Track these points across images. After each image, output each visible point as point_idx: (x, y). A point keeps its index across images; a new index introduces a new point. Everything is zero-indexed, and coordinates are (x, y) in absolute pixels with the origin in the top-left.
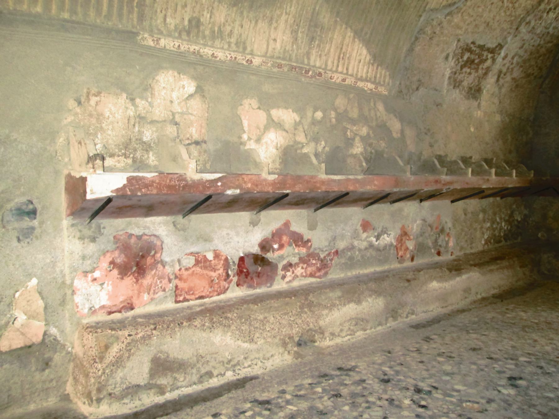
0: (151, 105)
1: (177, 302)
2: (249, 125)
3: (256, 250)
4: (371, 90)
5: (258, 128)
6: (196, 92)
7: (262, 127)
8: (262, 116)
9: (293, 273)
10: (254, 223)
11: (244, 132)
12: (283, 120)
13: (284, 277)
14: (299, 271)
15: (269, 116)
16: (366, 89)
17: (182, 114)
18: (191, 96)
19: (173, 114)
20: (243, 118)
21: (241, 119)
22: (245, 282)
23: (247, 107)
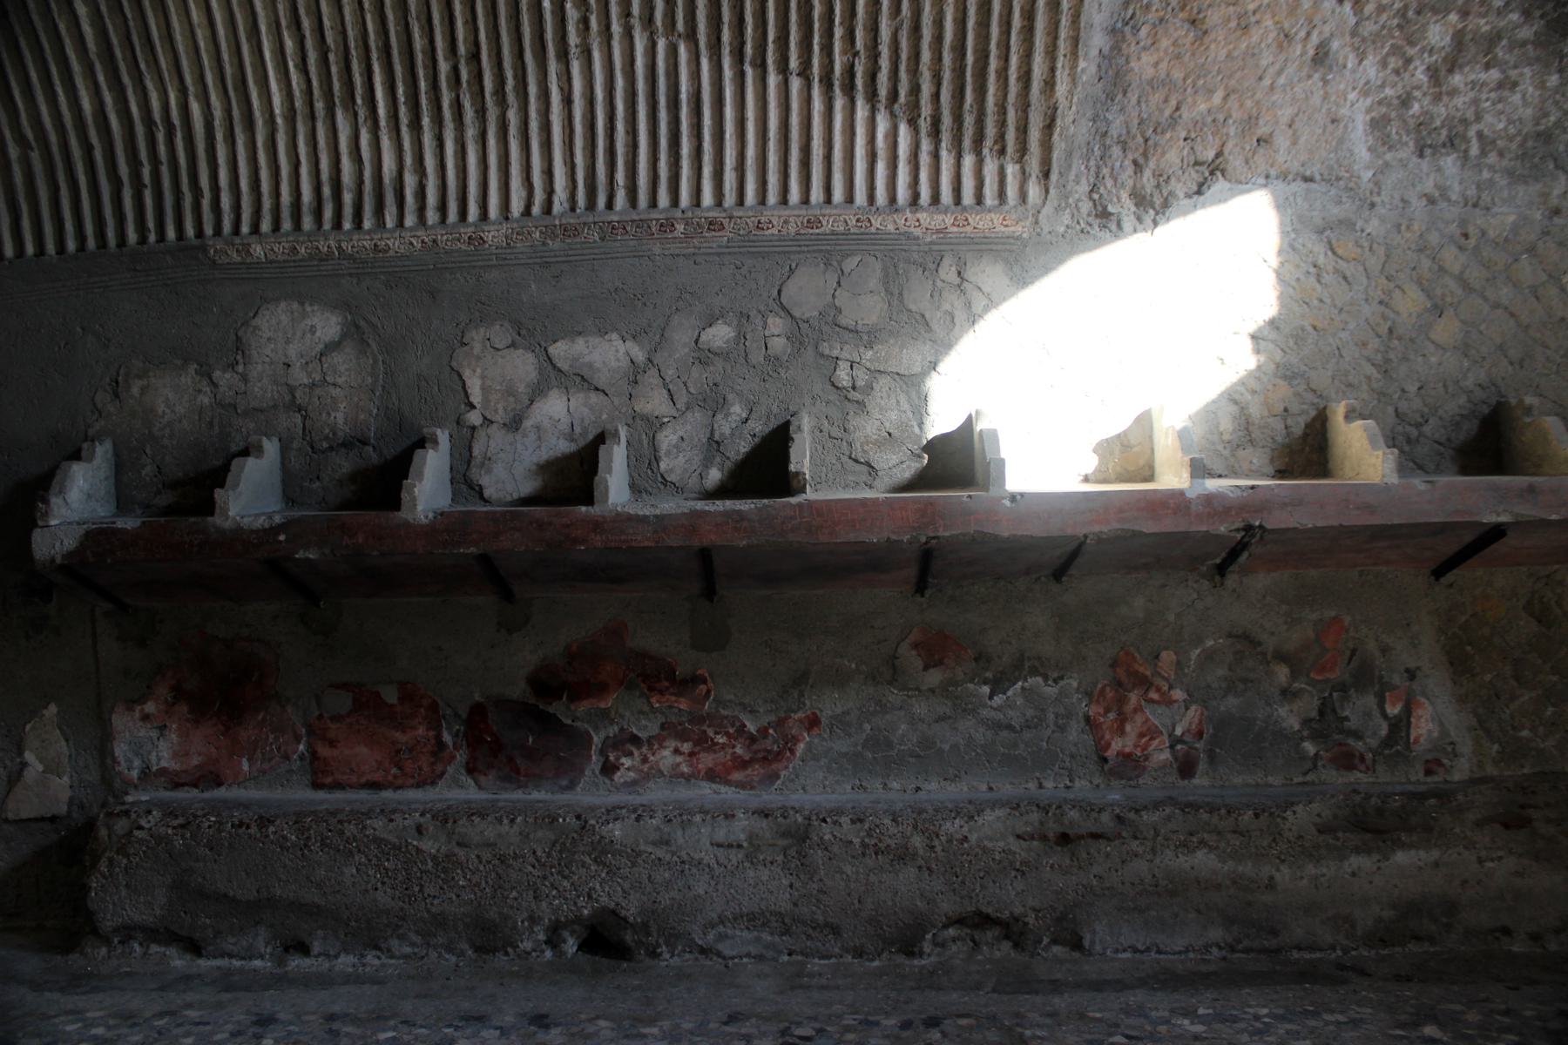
0: (245, 378)
2: (485, 390)
4: (938, 232)
6: (344, 336)
8: (522, 366)
9: (645, 760)
12: (590, 365)
13: (609, 769)
14: (666, 757)
16: (917, 232)
18: (332, 347)
19: (292, 390)
20: (467, 374)
21: (460, 376)
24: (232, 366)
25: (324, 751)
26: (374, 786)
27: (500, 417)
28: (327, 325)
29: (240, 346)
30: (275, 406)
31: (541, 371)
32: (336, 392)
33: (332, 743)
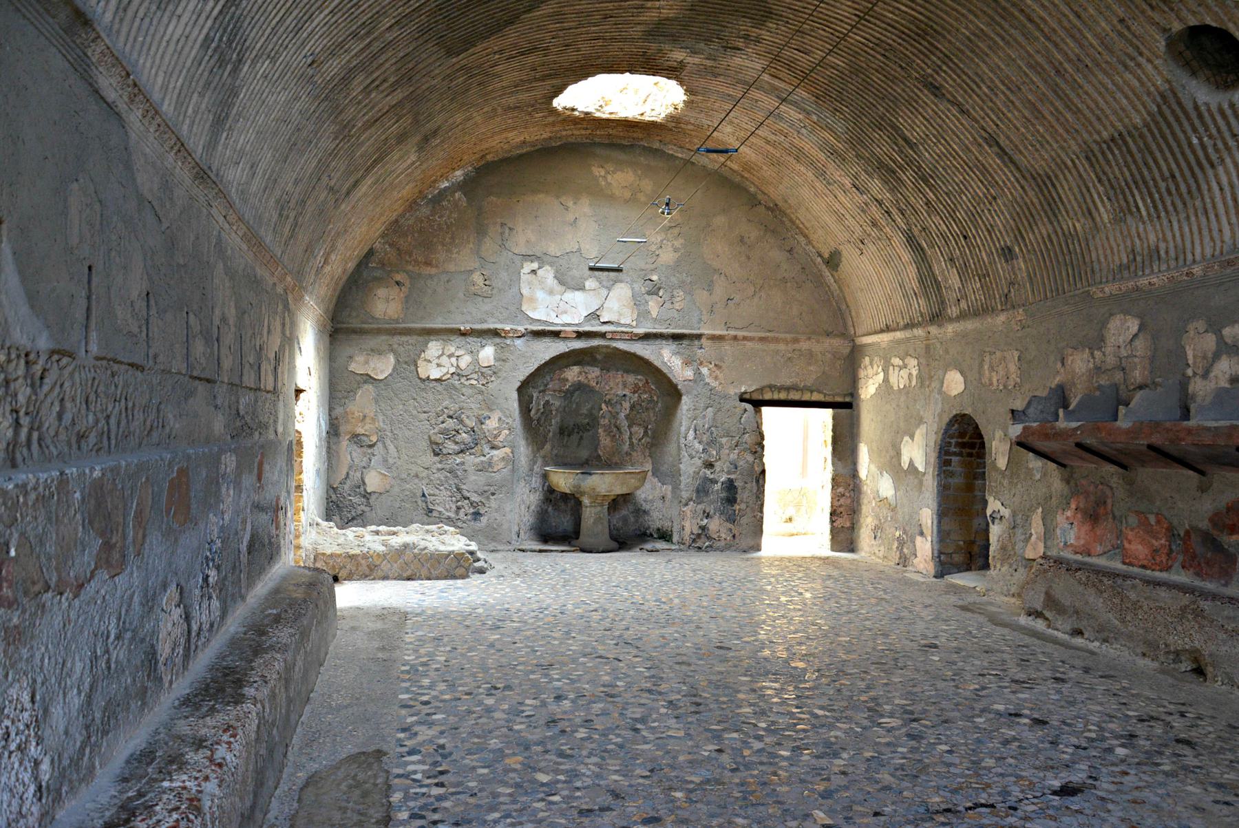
1: (1124, 563)
2: (1195, 357)
3: (1204, 525)
5: (1205, 357)
6: (1139, 330)
7: (1210, 355)
8: (1209, 342)
10: (1203, 489)
11: (1188, 365)
15: (1221, 339)
17: (1127, 357)
18: (1135, 336)
19: (1121, 359)
20: (1187, 347)
22: (1191, 566)
23: (1192, 333)
24: (1100, 349)
25: (1127, 545)
26: (1144, 567)
27: (1200, 371)
28: (1133, 325)
29: (1102, 339)
30: (1113, 368)
31: (1217, 344)
32: (1136, 360)
33: (1130, 542)
